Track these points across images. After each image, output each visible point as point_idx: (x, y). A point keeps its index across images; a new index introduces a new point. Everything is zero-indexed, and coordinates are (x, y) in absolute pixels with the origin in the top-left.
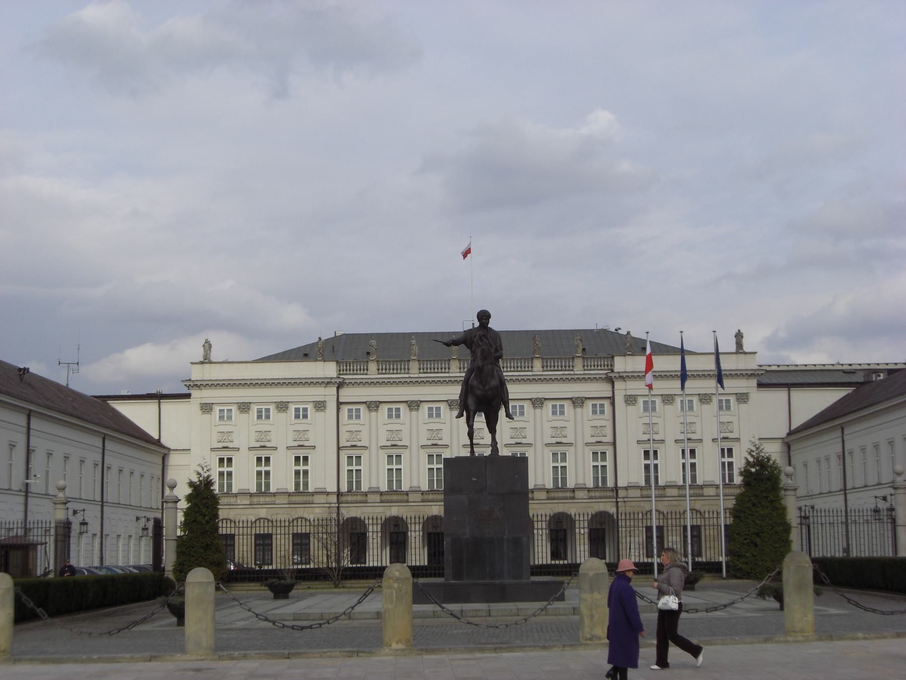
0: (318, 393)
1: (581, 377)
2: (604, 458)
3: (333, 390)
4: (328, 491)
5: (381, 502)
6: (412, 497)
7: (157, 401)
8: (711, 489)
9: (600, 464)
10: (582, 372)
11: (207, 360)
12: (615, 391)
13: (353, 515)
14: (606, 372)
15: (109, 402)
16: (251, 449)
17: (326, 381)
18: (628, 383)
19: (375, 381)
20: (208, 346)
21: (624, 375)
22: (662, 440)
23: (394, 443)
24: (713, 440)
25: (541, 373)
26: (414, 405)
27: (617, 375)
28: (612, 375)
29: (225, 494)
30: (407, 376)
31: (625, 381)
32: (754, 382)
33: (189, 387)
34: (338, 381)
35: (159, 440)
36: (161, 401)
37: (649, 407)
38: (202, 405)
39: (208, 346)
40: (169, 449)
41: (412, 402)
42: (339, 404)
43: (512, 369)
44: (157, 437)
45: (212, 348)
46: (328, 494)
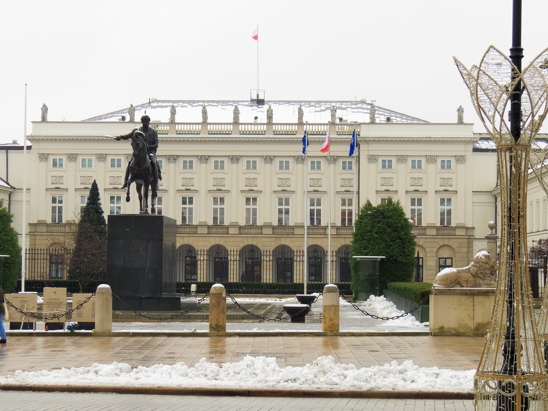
2: (350, 204)
6: (200, 230)
7: (5, 151)
8: (432, 230)
9: (347, 208)
11: (44, 120)
12: (360, 152)
16: (76, 190)
18: (370, 145)
19: (174, 139)
20: (45, 109)
21: (368, 139)
22: (396, 191)
23: (188, 188)
24: (435, 191)
26: (204, 159)
27: (362, 140)
29: (57, 224)
31: (369, 144)
32: (471, 148)
33: (30, 140)
36: (8, 151)
37: (387, 165)
38: (40, 155)
39: (45, 109)
40: (14, 188)
41: (202, 156)
45: (48, 112)
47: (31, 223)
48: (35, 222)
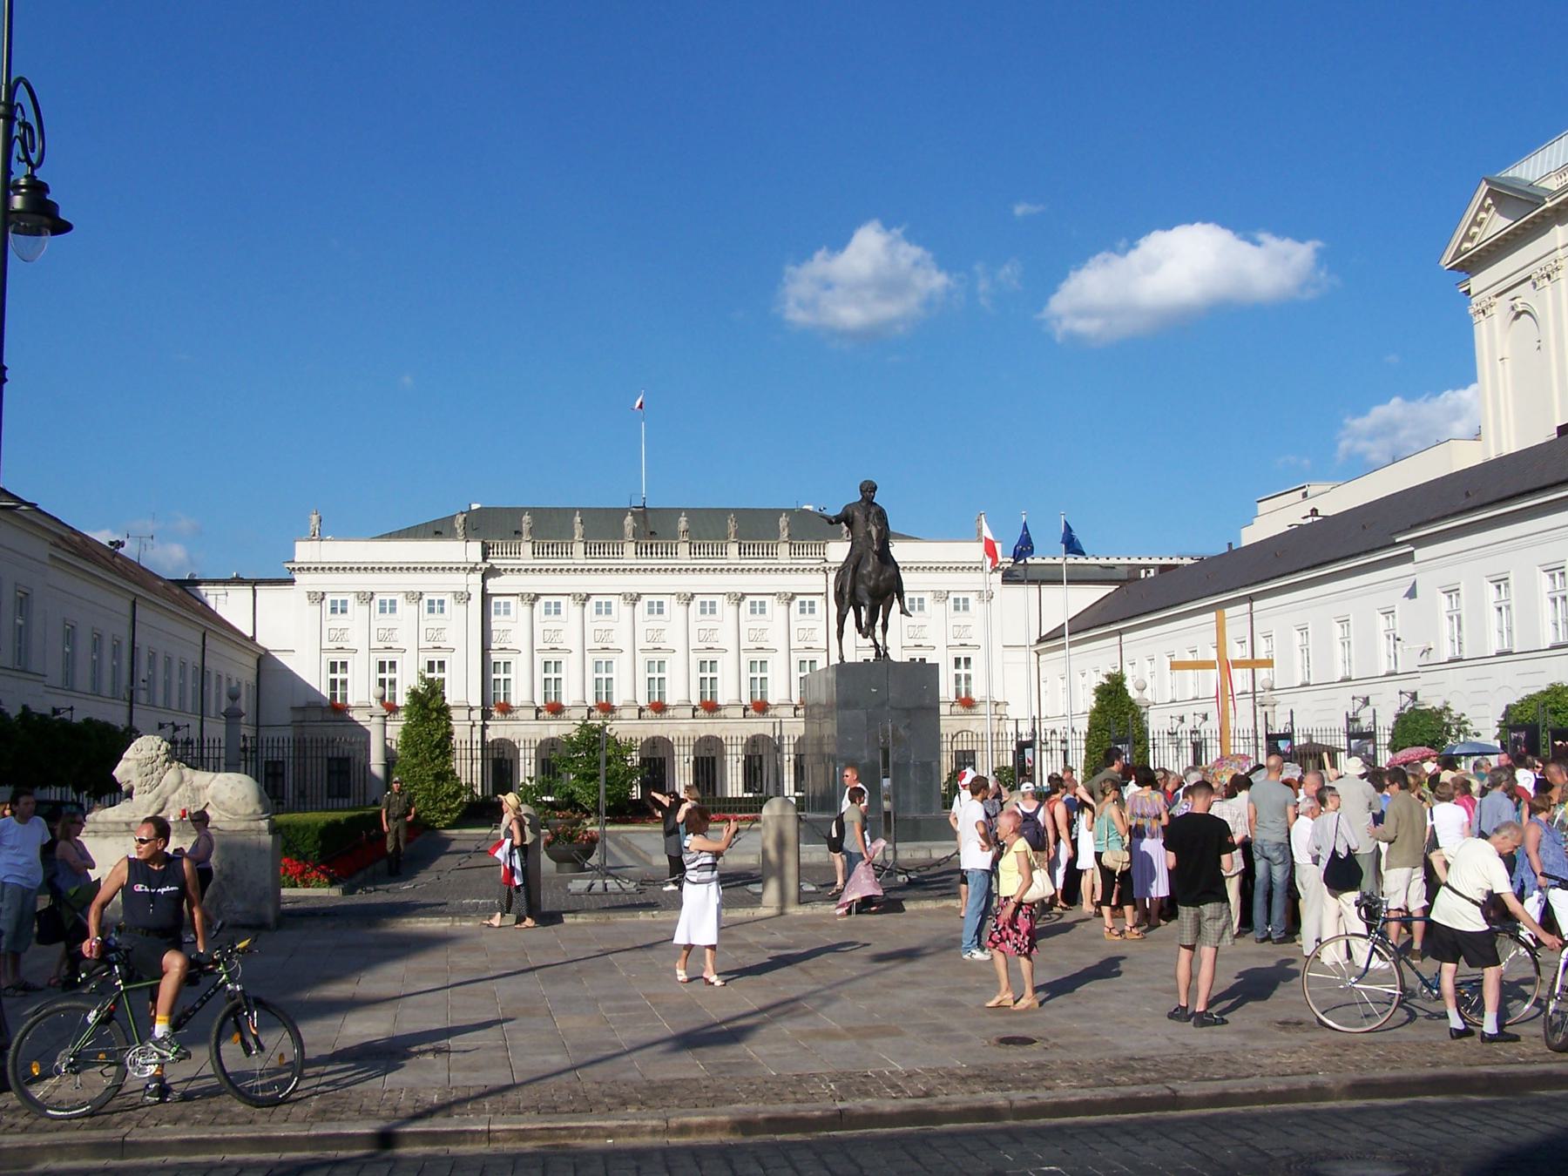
0: (459, 581)
1: (788, 567)
3: (478, 577)
4: (471, 705)
5: (537, 718)
10: (789, 562)
13: (501, 736)
14: (819, 561)
15: (187, 588)
17: (469, 566)
25: (738, 561)
28: (827, 566)
30: (571, 561)
34: (484, 566)
35: (253, 638)
42: (485, 597)
43: (702, 556)
44: (249, 634)
46: (471, 709)
47: (296, 706)
48: (302, 704)
